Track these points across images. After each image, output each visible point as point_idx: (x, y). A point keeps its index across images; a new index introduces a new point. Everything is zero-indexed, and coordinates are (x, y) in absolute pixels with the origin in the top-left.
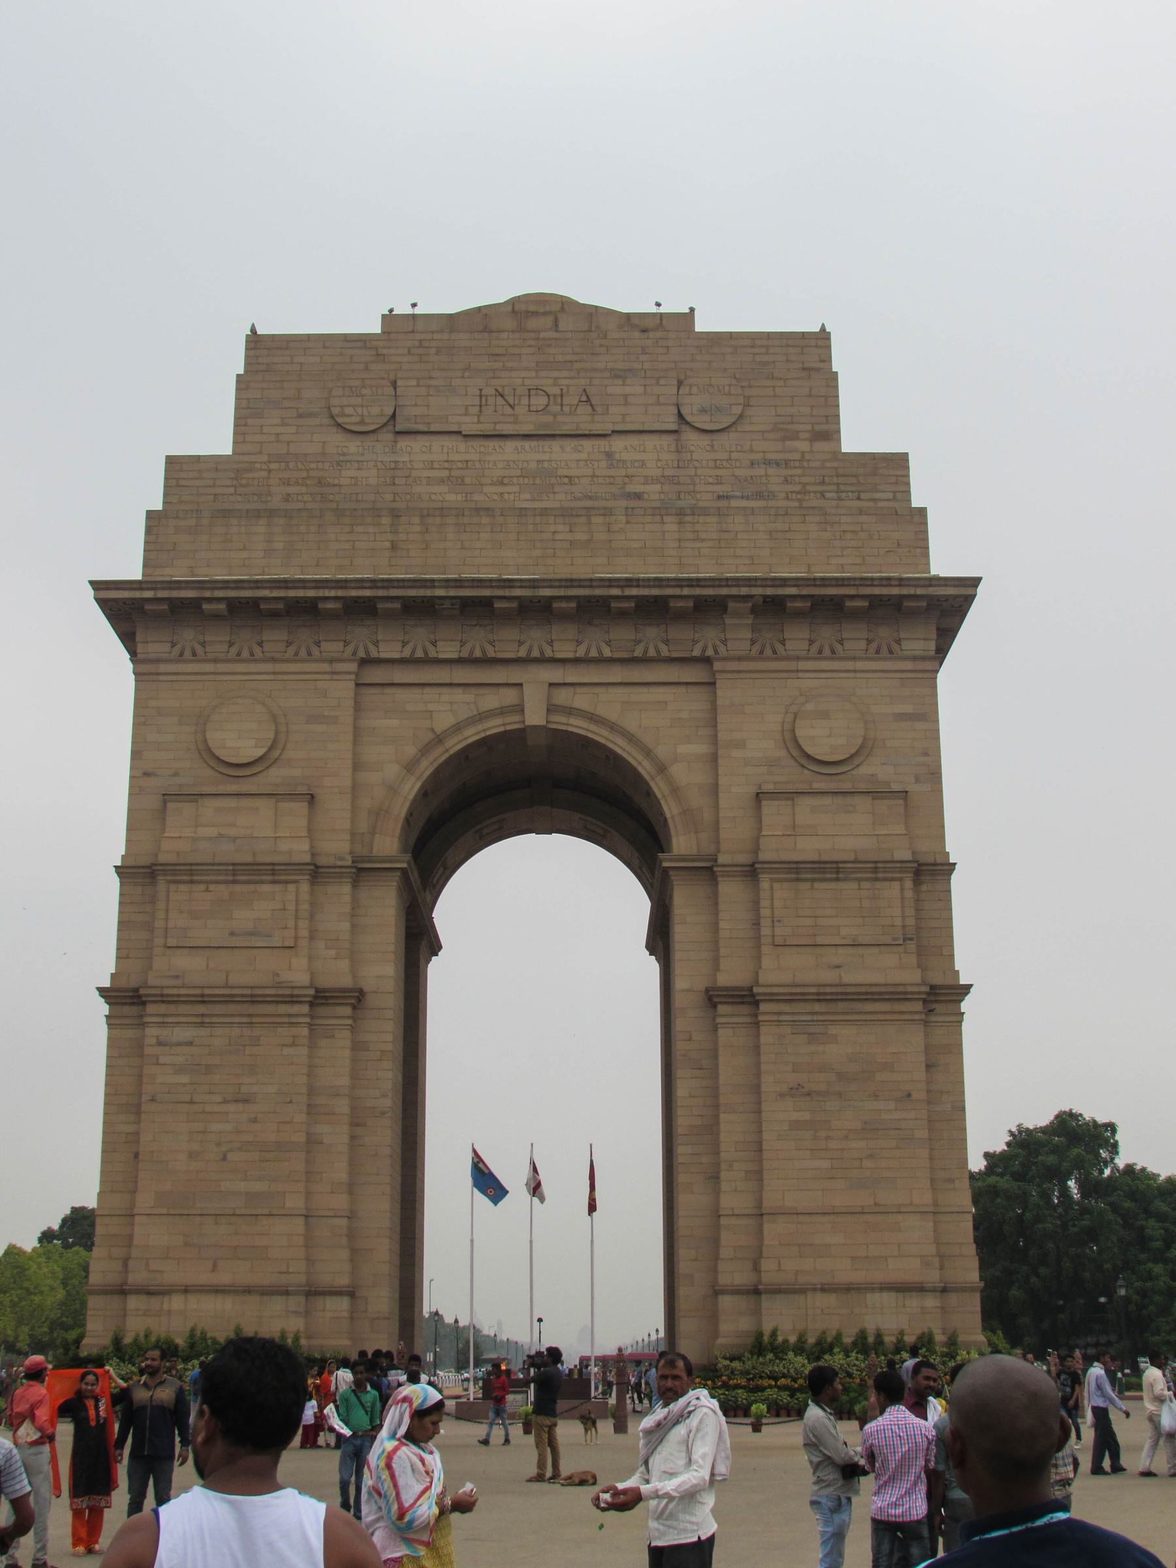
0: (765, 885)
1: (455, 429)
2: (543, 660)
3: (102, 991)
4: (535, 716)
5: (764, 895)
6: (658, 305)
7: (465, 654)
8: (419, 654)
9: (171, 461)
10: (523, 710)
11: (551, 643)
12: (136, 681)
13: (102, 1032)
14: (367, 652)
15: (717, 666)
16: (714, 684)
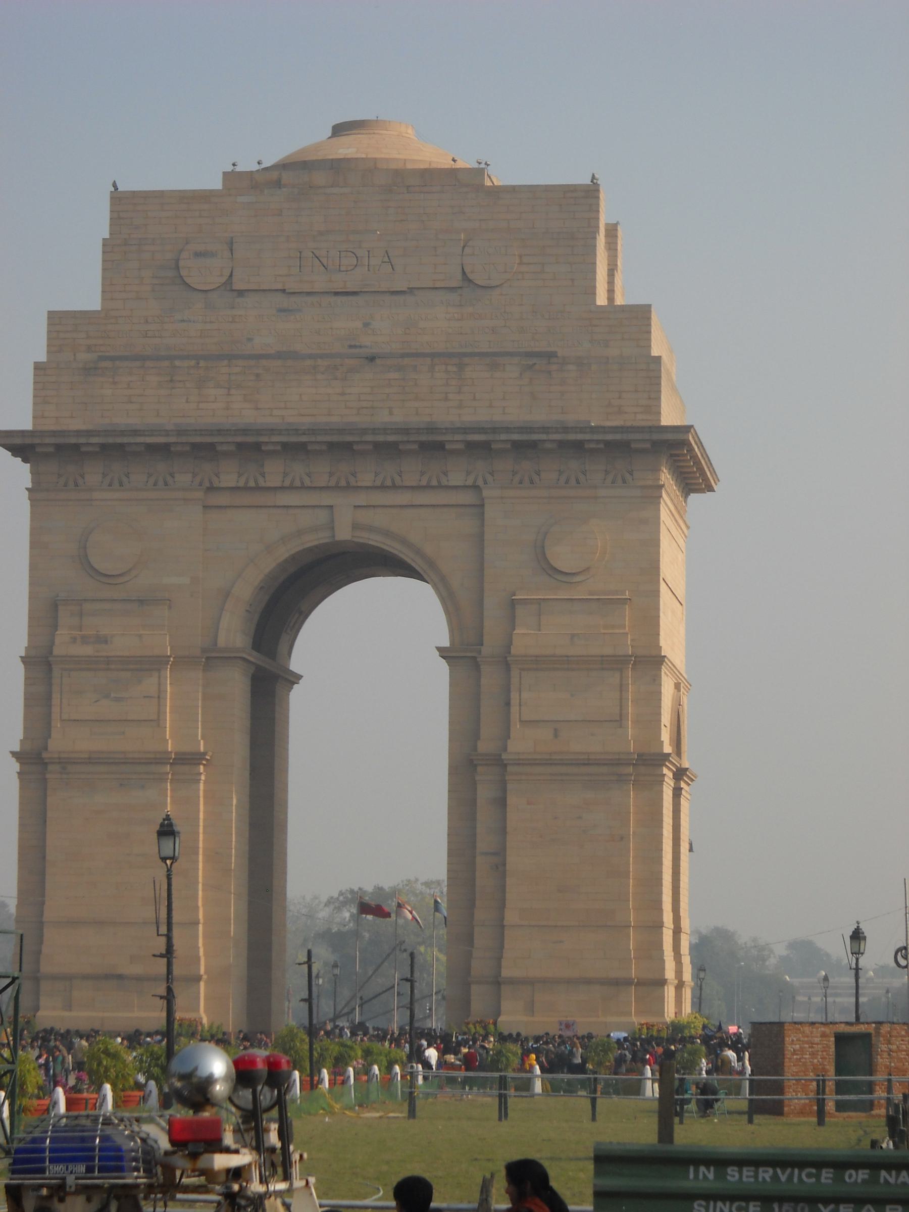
0: (515, 673)
1: (279, 287)
2: (348, 487)
3: (14, 754)
4: (344, 533)
5: (515, 680)
6: (454, 160)
7: (287, 483)
8: (252, 484)
9: (52, 315)
10: (333, 528)
11: (354, 474)
12: (31, 506)
13: (14, 784)
14: (211, 483)
15: (485, 493)
16: (483, 506)
